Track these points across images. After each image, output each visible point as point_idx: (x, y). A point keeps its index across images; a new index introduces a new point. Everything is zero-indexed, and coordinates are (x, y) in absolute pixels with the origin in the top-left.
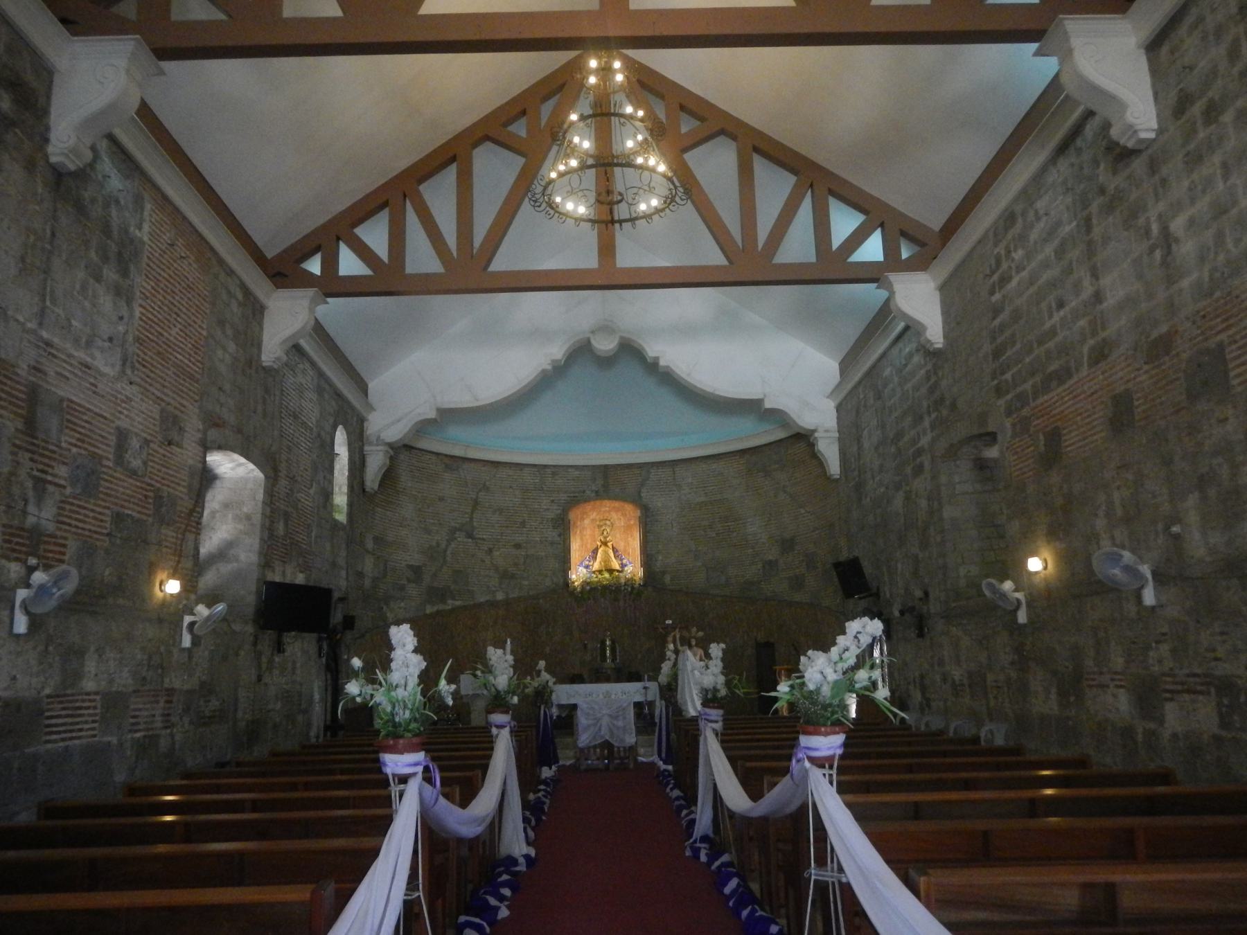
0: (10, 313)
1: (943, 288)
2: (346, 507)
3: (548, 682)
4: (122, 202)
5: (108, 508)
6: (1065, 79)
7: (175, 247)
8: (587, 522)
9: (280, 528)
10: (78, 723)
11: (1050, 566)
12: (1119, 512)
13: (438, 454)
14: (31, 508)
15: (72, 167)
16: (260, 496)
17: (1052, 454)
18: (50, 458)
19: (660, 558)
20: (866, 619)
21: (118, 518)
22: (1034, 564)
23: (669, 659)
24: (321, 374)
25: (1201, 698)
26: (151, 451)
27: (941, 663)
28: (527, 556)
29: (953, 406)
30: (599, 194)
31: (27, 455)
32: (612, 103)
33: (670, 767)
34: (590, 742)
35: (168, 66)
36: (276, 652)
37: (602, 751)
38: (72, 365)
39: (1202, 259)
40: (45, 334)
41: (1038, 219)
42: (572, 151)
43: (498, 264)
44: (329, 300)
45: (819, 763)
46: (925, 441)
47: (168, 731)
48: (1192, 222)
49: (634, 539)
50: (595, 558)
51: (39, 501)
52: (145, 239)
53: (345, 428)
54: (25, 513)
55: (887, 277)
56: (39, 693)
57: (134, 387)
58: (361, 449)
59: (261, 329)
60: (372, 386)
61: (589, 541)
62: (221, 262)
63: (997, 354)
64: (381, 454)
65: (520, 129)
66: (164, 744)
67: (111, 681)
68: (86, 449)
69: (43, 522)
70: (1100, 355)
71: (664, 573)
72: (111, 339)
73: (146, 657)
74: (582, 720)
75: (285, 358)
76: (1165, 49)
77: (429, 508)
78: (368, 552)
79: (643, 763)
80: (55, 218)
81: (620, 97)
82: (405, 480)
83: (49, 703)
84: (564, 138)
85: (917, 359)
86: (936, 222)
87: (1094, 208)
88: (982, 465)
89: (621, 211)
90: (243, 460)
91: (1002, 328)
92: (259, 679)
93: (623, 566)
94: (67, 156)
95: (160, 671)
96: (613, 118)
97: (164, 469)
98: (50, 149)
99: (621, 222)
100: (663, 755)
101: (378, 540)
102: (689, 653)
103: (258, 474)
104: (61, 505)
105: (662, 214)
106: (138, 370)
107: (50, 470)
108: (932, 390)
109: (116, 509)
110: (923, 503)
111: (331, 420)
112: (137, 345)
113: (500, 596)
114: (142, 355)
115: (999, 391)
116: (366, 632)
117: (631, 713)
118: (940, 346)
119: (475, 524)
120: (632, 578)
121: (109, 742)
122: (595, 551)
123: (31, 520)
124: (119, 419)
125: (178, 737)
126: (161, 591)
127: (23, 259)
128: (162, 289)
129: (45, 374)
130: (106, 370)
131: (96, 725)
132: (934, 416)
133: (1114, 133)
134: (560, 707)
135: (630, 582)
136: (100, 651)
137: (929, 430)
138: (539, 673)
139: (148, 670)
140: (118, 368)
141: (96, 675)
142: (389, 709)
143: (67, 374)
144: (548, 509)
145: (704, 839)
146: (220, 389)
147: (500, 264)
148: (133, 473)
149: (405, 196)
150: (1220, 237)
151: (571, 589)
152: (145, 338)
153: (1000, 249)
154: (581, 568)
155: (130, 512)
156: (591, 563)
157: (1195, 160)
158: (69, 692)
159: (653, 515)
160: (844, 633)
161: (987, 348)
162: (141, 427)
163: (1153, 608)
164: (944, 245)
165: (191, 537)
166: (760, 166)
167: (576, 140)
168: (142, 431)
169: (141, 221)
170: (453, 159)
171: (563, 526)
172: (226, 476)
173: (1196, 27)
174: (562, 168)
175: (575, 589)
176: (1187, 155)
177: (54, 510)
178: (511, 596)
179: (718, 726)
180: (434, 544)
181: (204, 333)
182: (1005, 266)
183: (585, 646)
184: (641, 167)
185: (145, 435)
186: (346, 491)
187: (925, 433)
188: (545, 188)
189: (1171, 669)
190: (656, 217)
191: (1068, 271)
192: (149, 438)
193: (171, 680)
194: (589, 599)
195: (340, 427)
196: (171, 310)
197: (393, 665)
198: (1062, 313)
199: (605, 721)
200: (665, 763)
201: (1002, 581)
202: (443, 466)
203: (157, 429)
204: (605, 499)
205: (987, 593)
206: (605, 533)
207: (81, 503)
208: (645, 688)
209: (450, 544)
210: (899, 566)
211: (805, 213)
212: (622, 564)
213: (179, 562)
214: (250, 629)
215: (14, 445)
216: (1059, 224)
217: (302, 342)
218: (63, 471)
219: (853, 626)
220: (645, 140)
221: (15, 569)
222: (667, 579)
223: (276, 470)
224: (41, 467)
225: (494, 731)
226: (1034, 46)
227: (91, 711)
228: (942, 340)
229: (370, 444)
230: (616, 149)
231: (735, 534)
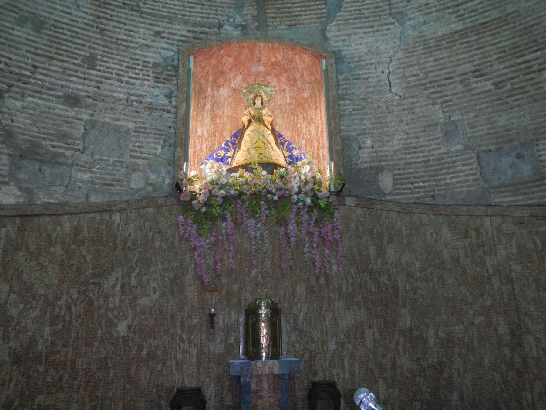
8: (224, 92)
19: (369, 142)
28: (91, 125)
49: (310, 123)
61: (228, 127)
93: (293, 160)
120: (314, 178)
122: (239, 135)
144: (148, 46)
151: (183, 197)
156: (229, 154)
159: (351, 70)
175: (194, 196)
178: (42, 198)
194: (225, 219)
204: (258, 39)
206: (258, 101)
212: (291, 156)
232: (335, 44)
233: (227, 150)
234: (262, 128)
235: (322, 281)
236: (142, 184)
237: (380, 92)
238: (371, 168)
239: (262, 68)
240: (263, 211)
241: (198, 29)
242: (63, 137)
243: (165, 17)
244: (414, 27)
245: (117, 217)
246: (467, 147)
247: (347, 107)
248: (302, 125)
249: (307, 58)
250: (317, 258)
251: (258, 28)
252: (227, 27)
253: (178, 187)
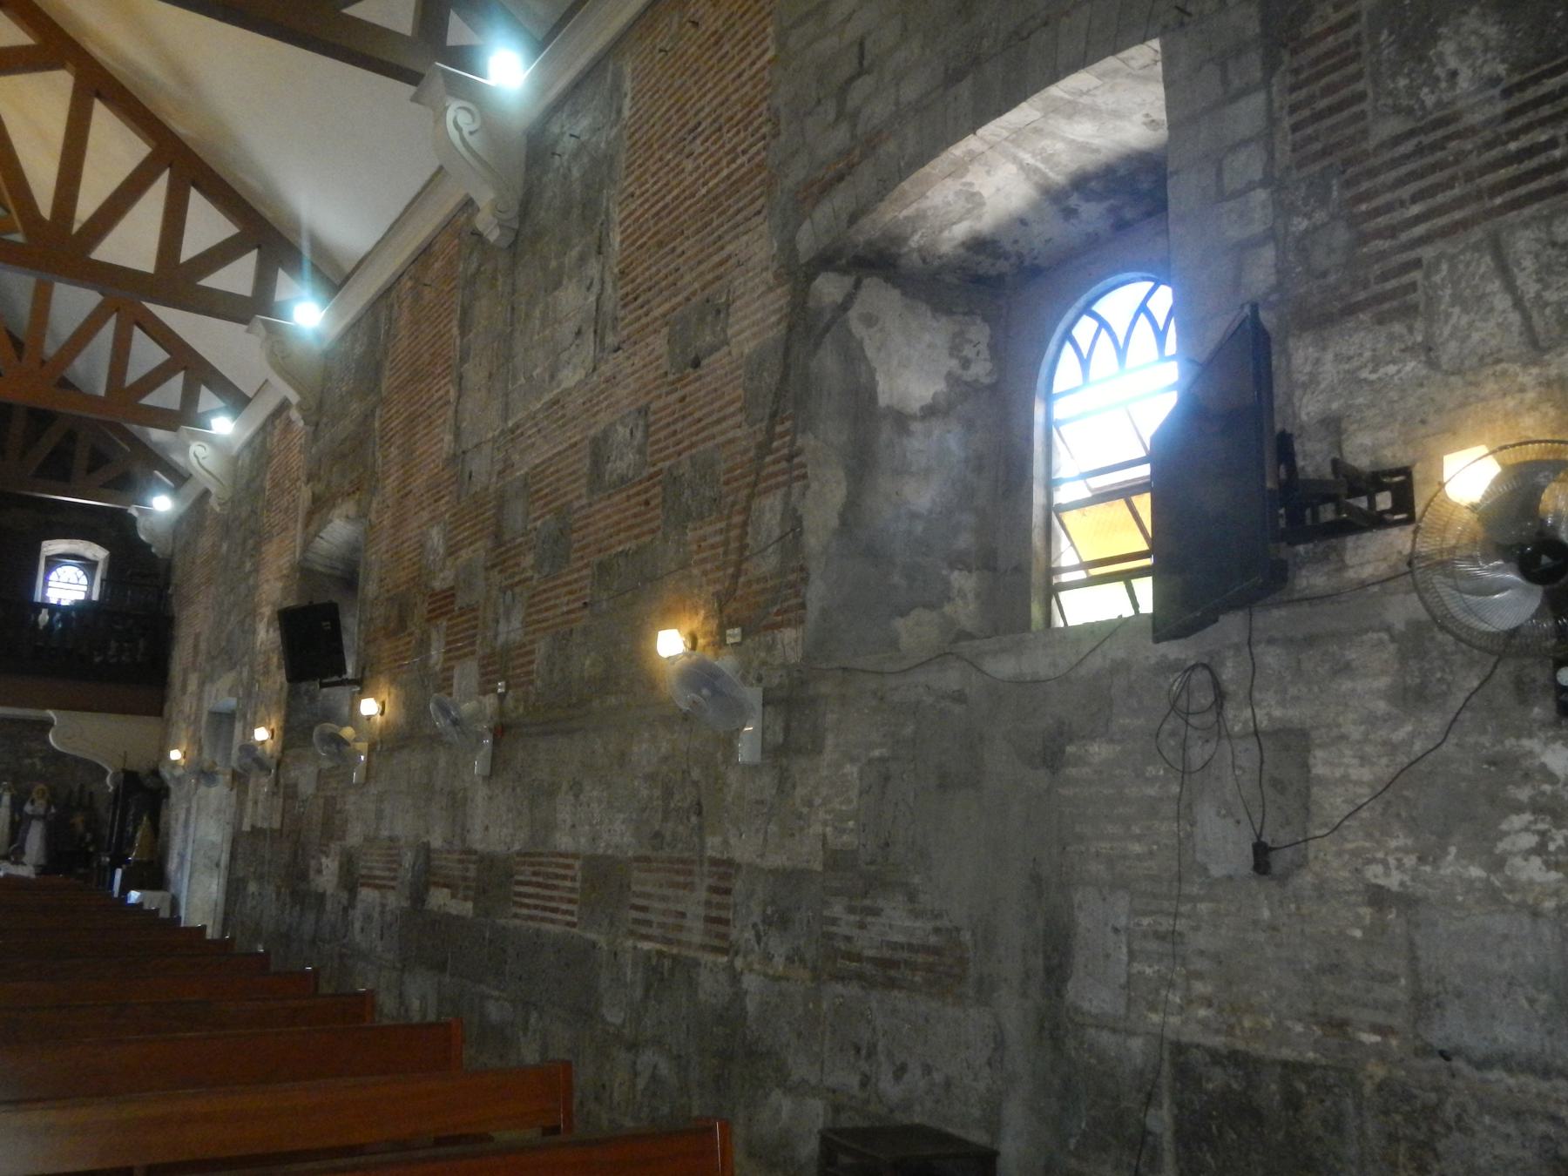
10: (551, 898)
66: (711, 986)
73: (657, 793)
95: (694, 819)
121: (594, 945)
125: (751, 982)
136: (576, 788)
139: (665, 819)
141: (573, 826)
158: (540, 849)
193: (726, 842)
227: (568, 884)
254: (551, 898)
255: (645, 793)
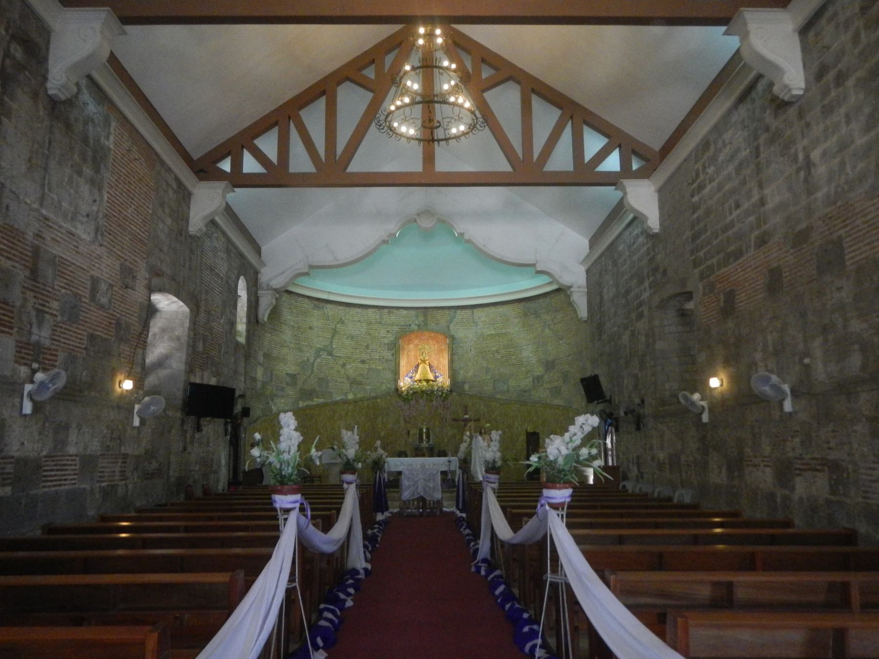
0: (21, 197)
1: (660, 191)
2: (245, 333)
3: (382, 455)
4: (96, 121)
5: (85, 330)
6: (745, 54)
7: (131, 152)
8: (411, 346)
9: (200, 347)
10: (65, 475)
11: (725, 384)
12: (771, 349)
13: (309, 297)
14: (35, 330)
15: (63, 98)
16: (187, 324)
17: (728, 309)
18: (48, 296)
19: (462, 372)
20: (588, 415)
21: (92, 337)
22: (714, 382)
23: (465, 442)
24: (229, 240)
25: (819, 474)
26: (114, 293)
27: (651, 449)
28: (369, 369)
29: (665, 273)
30: (424, 122)
31: (32, 294)
32: (434, 59)
33: (464, 515)
34: (410, 497)
35: (129, 28)
36: (196, 431)
37: (418, 503)
38: (62, 233)
39: (830, 180)
40: (44, 212)
41: (725, 146)
42: (406, 91)
43: (353, 168)
44: (236, 189)
45: (555, 507)
46: (645, 296)
47: (124, 482)
48: (824, 154)
50: (416, 372)
51: (40, 324)
52: (112, 147)
53: (245, 278)
54: (30, 333)
55: (621, 182)
56: (39, 454)
57: (103, 248)
58: (256, 293)
59: (189, 208)
60: (264, 249)
61: (413, 360)
62: (162, 163)
63: (695, 238)
64: (270, 296)
65: (370, 73)
66: (120, 491)
67: (86, 448)
68: (71, 291)
69: (42, 339)
70: (762, 241)
71: (464, 383)
72: (88, 216)
73: (109, 432)
74: (405, 482)
75: (204, 229)
76: (811, 34)
77: (302, 333)
78: (259, 363)
79: (446, 512)
80: (51, 133)
81: (439, 54)
82: (287, 315)
83: (45, 461)
84: (401, 82)
85: (641, 239)
86: (657, 145)
87: (762, 140)
88: (683, 314)
89: (439, 134)
90: (175, 299)
91: (699, 220)
92: (185, 449)
93: (436, 377)
94: (59, 89)
95: (118, 441)
96: (435, 69)
97: (122, 305)
98: (49, 85)
99: (439, 141)
100: (460, 507)
101: (267, 356)
102: (480, 438)
103: (186, 309)
104: (55, 328)
105: (467, 136)
106: (106, 236)
107: (47, 304)
108: (652, 260)
109: (90, 331)
110: (643, 339)
111: (236, 272)
112: (105, 219)
113: (350, 396)
114: (109, 227)
115: (696, 264)
116: (258, 419)
117: (439, 478)
118: (657, 231)
119: (334, 346)
120: (442, 386)
121: (84, 489)
122: (417, 366)
123: (34, 338)
124: (93, 270)
125: (130, 486)
126: (120, 387)
127: (30, 160)
128: (122, 181)
129: (44, 239)
130: (84, 236)
131: (76, 477)
132: (651, 279)
133: (776, 89)
134: (390, 473)
135: (440, 390)
136: (79, 427)
137: (648, 289)
138: (376, 449)
139: (111, 441)
140: (93, 234)
141: (76, 443)
142: (278, 466)
143: (59, 240)
144: (385, 337)
145: (484, 560)
146: (161, 250)
147: (355, 166)
148: (102, 307)
149: (290, 118)
150: (843, 164)
152: (110, 215)
153: (699, 165)
154: (407, 378)
155: (99, 334)
156: (414, 375)
157: (827, 111)
158: (59, 454)
160: (573, 424)
161: (688, 234)
162: (107, 276)
163: (790, 414)
164: (662, 161)
165: (140, 351)
166: (537, 104)
167: (409, 83)
168: (109, 278)
169: (109, 134)
170: (323, 93)
171: (395, 348)
172: (164, 310)
173: (832, 20)
174: (399, 103)
175: (402, 392)
176: (824, 106)
177: (50, 332)
178: (359, 396)
179: (496, 486)
180: (305, 359)
181: (150, 211)
182: (702, 177)
183: (408, 432)
184: (454, 104)
185: (110, 282)
186: (245, 321)
187: (645, 290)
188: (387, 117)
189: (801, 455)
190: (463, 138)
191: (744, 183)
192: (114, 283)
194: (412, 399)
195: (242, 277)
196: (128, 195)
197: (282, 438)
198: (738, 211)
199: (421, 484)
200: (461, 512)
201: (692, 393)
202: (313, 305)
203: (118, 277)
205: (682, 401)
206: (424, 354)
207: (67, 327)
208: (449, 461)
209: (316, 359)
210: (626, 381)
211: (567, 135)
212: (435, 376)
213: (132, 368)
214: (179, 415)
215: (24, 287)
216: (738, 150)
217: (217, 219)
218: (55, 305)
219: (580, 420)
220: (456, 85)
221: (23, 371)
222: (467, 387)
223: (198, 307)
224: (41, 302)
225: (345, 486)
226: (723, 29)
227: (73, 467)
228: (658, 227)
229: (263, 289)
230: (437, 90)
231: (514, 357)
232: (453, 332)
233: (413, 374)
234: (425, 365)
235: (444, 420)
236: (385, 388)
237: (467, 353)
238: (462, 382)
239: (426, 337)
240: (425, 396)
241: (402, 327)
242: (361, 375)
243: (390, 324)
244: (480, 329)
245: (379, 400)
246: (491, 378)
247: (456, 358)
248: (441, 359)
249: (442, 336)
250: (442, 413)
251: (424, 326)
252: (412, 325)
253: (397, 390)
254: (65, 475)
255: (105, 431)
